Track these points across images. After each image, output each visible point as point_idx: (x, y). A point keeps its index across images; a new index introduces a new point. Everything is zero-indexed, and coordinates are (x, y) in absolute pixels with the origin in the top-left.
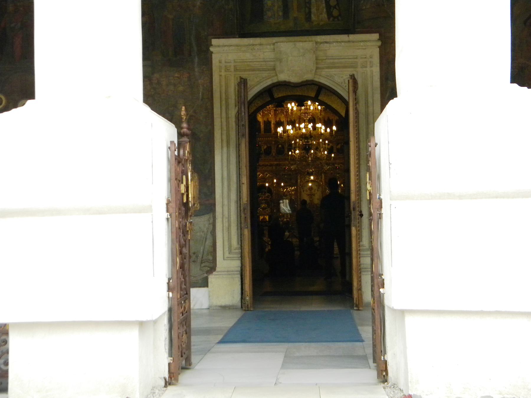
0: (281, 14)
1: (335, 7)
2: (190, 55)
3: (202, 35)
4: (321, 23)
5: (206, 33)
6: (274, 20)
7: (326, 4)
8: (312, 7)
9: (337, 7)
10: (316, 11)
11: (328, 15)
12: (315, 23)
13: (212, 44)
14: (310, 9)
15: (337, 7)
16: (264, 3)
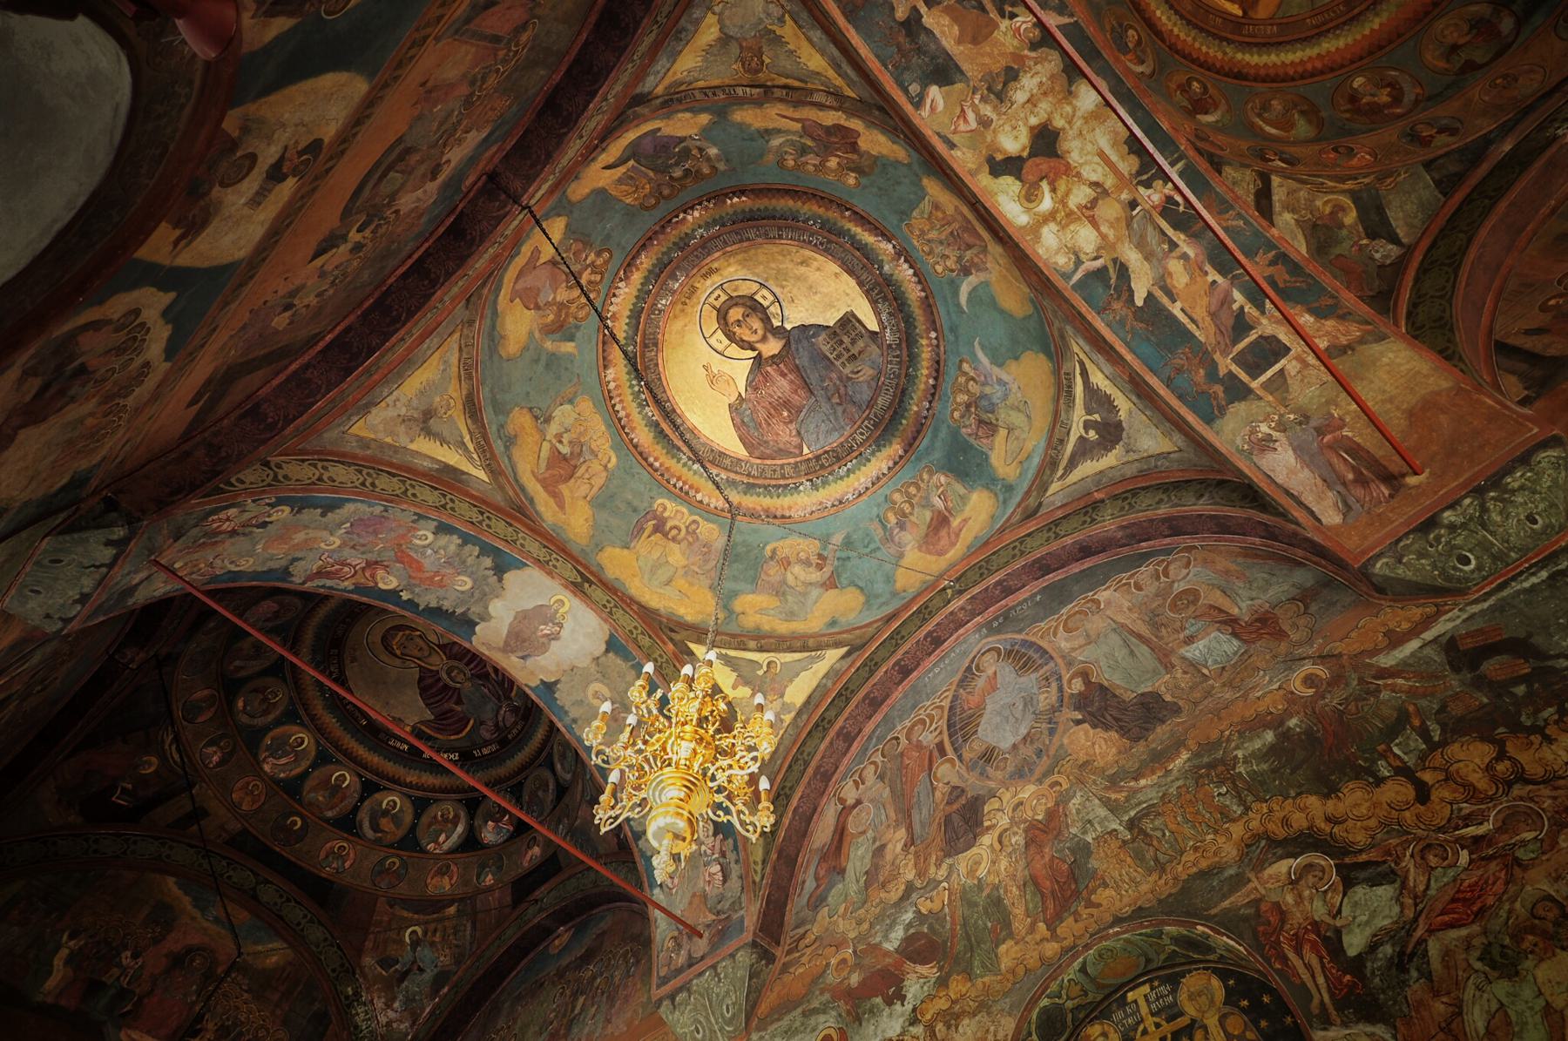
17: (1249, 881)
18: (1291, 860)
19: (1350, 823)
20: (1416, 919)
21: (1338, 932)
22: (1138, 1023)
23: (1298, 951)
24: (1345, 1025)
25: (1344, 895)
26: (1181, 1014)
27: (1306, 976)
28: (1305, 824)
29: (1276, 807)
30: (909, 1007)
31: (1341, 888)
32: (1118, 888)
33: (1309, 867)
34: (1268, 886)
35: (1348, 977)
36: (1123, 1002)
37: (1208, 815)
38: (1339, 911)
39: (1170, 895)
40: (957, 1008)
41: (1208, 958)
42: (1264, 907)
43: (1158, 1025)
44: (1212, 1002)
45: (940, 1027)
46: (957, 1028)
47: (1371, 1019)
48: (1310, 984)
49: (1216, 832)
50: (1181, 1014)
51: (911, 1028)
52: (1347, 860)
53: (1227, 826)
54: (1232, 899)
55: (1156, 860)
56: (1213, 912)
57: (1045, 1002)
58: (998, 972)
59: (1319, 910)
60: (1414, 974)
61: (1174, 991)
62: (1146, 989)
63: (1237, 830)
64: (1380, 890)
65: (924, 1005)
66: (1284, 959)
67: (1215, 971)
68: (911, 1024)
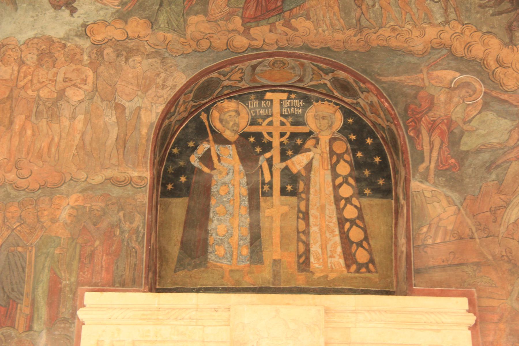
0: (245, 251)
1: (360, 244)
2: (30, 328)
3: (64, 282)
4: (332, 276)
5: (73, 279)
6: (229, 263)
7: (341, 238)
8: (311, 242)
9: (365, 244)
10: (320, 251)
11: (346, 259)
12: (318, 275)
13: (85, 303)
14: (307, 245)
15: (365, 244)
16: (209, 228)
17: (421, 72)
18: (457, 74)
19: (510, 70)
20: (514, 148)
21: (462, 133)
22: (268, 116)
23: (431, 131)
24: (435, 184)
25: (480, 113)
26: (304, 124)
27: (426, 148)
28: (481, 55)
29: (467, 33)
30: (78, 20)
31: (480, 108)
32: (317, 24)
33: (467, 84)
34: (432, 82)
35: (453, 161)
36: (261, 97)
37: (415, 10)
38: (470, 121)
39: (357, 52)
40: (131, 44)
41: (345, 99)
42: (421, 94)
43: (282, 124)
44: (331, 126)
45: (108, 51)
46: (127, 59)
47: (452, 188)
48: (426, 154)
49: (415, 26)
50: (304, 124)
51: (77, 39)
52: (494, 94)
53: (425, 26)
54: (402, 78)
55: (359, 20)
56: (384, 79)
57: (214, 75)
58: (183, 34)
59: (457, 114)
60: (494, 176)
61: (305, 108)
62: (284, 96)
63: (431, 33)
64: (503, 121)
65: (95, 26)
66: (418, 132)
67: (342, 108)
68: (79, 36)
